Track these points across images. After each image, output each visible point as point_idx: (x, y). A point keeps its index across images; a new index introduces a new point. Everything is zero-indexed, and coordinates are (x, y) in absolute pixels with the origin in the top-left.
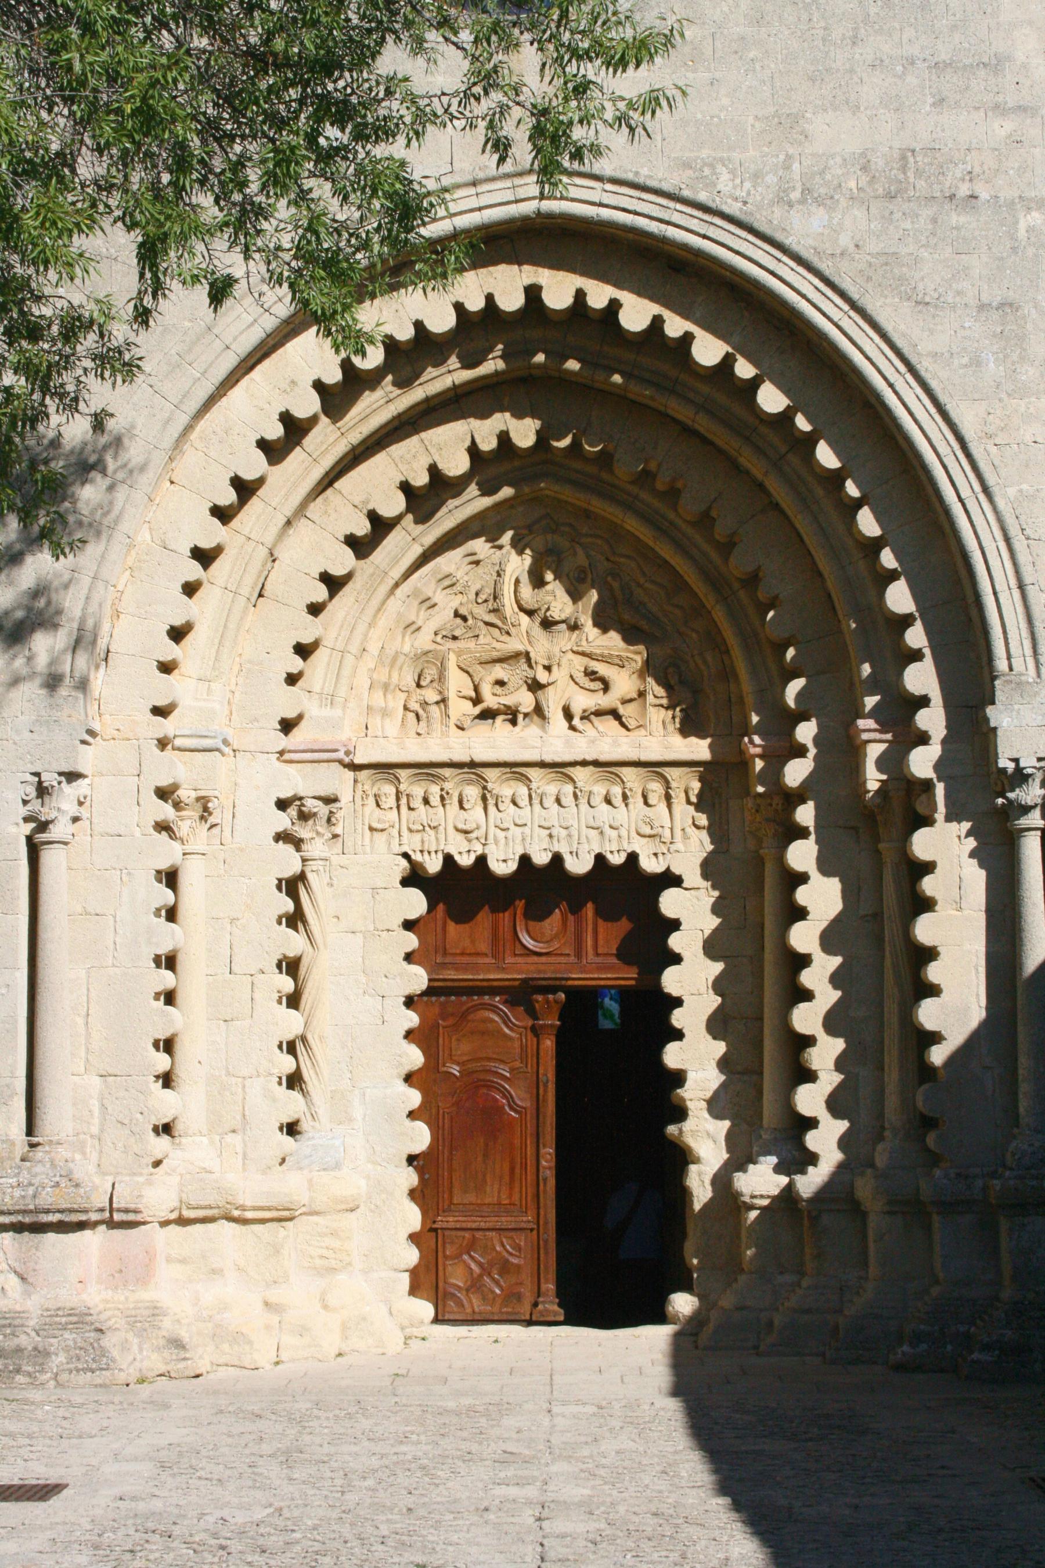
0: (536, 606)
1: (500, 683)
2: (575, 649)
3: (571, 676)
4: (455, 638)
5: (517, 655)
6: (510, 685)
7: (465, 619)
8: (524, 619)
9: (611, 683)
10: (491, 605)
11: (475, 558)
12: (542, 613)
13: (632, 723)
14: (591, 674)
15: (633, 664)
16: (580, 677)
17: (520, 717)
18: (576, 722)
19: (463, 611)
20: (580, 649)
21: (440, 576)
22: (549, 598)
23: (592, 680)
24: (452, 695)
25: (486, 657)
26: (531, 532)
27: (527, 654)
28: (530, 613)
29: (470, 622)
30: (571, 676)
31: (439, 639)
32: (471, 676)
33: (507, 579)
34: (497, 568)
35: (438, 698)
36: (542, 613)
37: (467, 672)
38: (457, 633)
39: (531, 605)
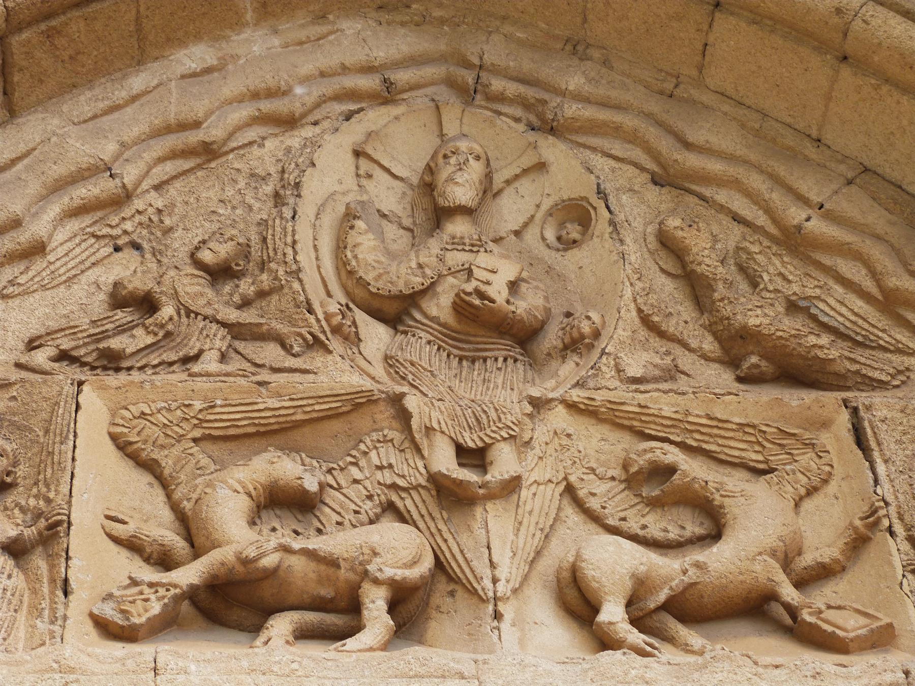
0: (417, 281)
1: (284, 502)
2: (576, 395)
3: (570, 490)
4: (112, 361)
5: (358, 403)
6: (328, 515)
7: (147, 304)
8: (376, 336)
9: (733, 507)
10: (246, 287)
11: (193, 138)
12: (440, 306)
13: (851, 625)
14: (652, 482)
15: (806, 459)
16: (602, 493)
17: (376, 604)
18: (612, 613)
19: (139, 284)
20: (600, 396)
21: (59, 170)
22: (457, 258)
23: (654, 504)
24: (85, 518)
25: (225, 416)
26: (388, 95)
27: (397, 400)
28: (396, 311)
29: (167, 311)
30: (570, 490)
31: (41, 357)
32: (165, 483)
33: (307, 209)
34: (269, 189)
35: (30, 533)
36: (440, 306)
37: (149, 466)
38: (115, 343)
39: (403, 276)
